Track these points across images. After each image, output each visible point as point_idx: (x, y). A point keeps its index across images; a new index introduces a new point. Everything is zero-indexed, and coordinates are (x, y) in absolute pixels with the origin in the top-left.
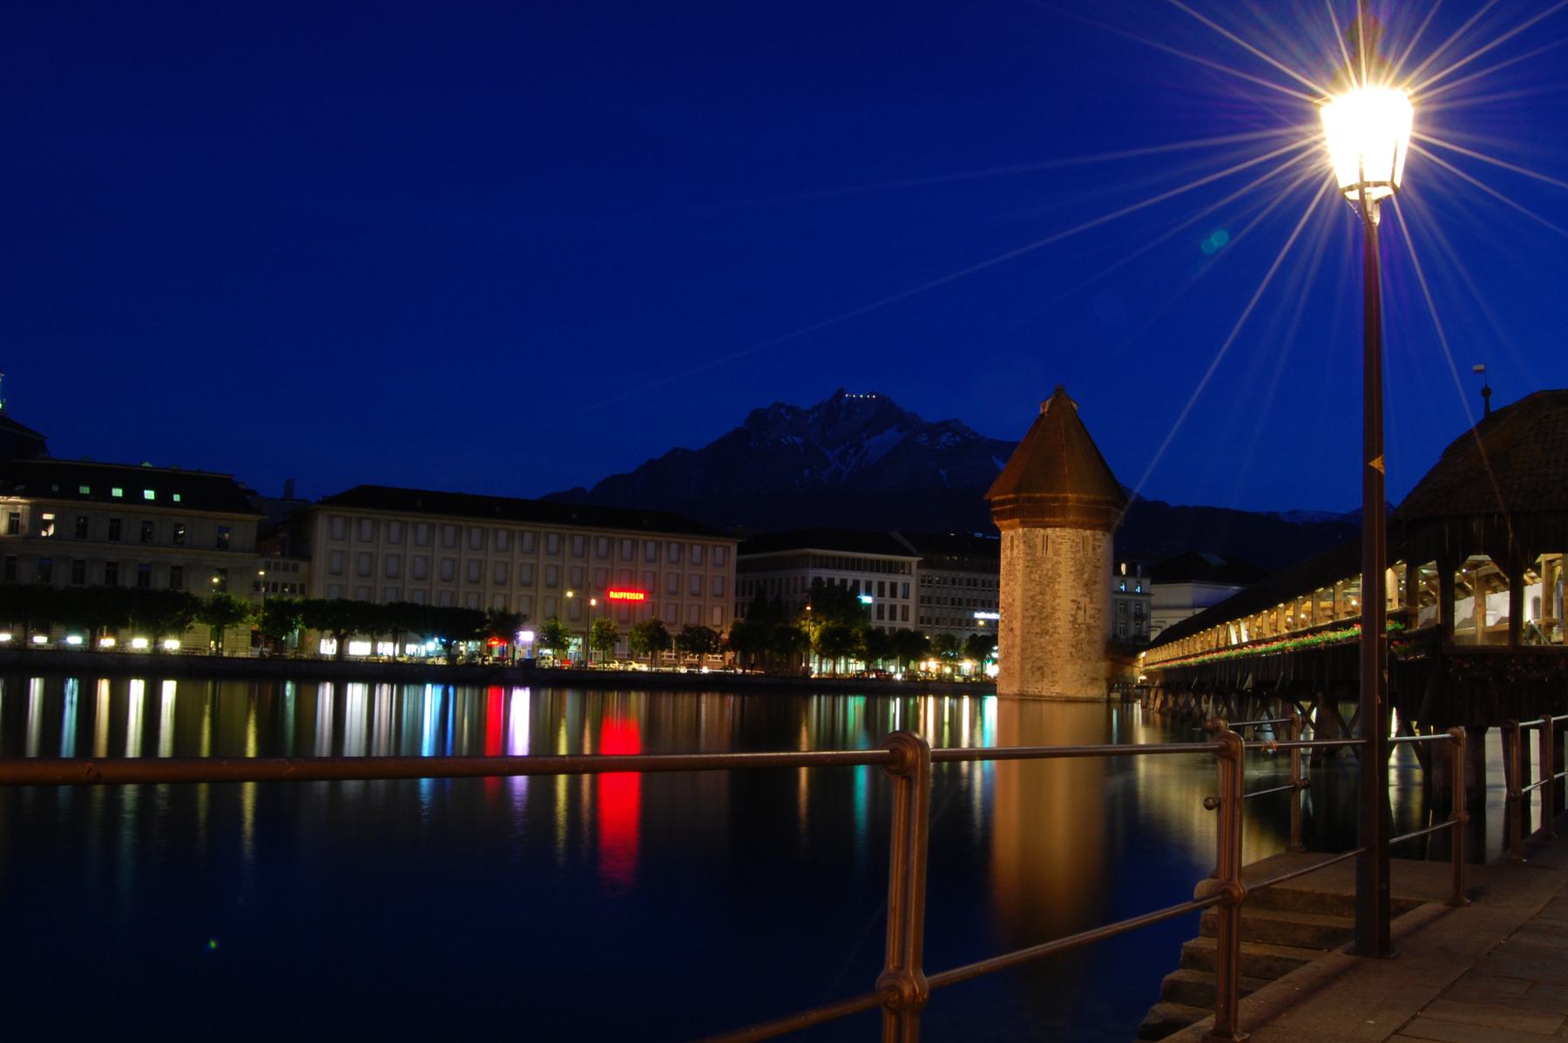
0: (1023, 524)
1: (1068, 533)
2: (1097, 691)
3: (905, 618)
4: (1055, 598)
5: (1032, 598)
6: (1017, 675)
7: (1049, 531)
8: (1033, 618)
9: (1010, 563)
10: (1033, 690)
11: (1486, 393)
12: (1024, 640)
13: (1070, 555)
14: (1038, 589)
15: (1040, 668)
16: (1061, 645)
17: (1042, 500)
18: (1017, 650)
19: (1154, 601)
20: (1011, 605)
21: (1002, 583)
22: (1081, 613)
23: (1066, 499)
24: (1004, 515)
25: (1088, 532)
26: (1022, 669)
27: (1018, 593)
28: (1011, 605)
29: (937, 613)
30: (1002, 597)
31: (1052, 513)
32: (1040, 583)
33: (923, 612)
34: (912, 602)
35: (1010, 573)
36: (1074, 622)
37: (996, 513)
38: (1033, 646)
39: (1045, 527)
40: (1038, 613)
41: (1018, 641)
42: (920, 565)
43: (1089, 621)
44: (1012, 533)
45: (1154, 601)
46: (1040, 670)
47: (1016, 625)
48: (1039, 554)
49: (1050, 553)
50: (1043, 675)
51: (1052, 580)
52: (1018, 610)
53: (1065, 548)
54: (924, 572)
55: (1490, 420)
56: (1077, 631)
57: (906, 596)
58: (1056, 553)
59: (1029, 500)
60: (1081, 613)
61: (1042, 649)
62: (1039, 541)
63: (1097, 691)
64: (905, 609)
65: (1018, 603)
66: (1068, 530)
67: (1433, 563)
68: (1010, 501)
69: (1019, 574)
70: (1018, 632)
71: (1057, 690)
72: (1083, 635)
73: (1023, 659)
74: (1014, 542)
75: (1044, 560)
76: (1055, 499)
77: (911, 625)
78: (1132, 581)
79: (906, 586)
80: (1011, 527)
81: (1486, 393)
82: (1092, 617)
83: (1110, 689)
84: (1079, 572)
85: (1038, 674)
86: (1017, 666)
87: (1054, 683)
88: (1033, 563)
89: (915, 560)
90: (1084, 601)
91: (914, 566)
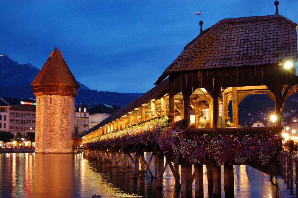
0: (44, 94)
1: (59, 97)
2: (69, 150)
3: (5, 127)
4: (54, 119)
5: (47, 119)
6: (42, 146)
7: (53, 96)
8: (47, 126)
9: (39, 108)
10: (47, 151)
11: (201, 23)
12: (44, 134)
13: (60, 104)
14: (49, 116)
15: (50, 143)
16: (56, 135)
17: (50, 86)
18: (42, 137)
19: (90, 120)
20: (39, 122)
21: (37, 114)
22: (64, 124)
23: (58, 86)
24: (37, 91)
25: (66, 97)
26: (44, 144)
27: (42, 118)
28: (39, 122)
29: (17, 125)
30: (36, 119)
31: (54, 90)
32: (50, 114)
33: (11, 125)
34: (7, 122)
35: (39, 110)
36: (61, 127)
37: (34, 90)
38: (47, 136)
39: (51, 95)
40: (49, 125)
41: (42, 134)
42: (10, 109)
43: (66, 126)
44: (40, 97)
46: (50, 144)
47: (41, 128)
48: (49, 104)
49: (53, 103)
50: (51, 145)
51: (54, 113)
52: (42, 123)
53: (58, 102)
54: (12, 111)
55: (203, 33)
56: (62, 130)
57: (5, 119)
58: (55, 104)
59: (46, 86)
60: (64, 124)
61: (50, 136)
62: (49, 100)
63: (69, 150)
64: (5, 124)
65: (42, 121)
66: (59, 96)
67: (181, 93)
68: (39, 86)
69: (42, 111)
70: (42, 131)
71: (55, 150)
72: (64, 131)
75: (51, 106)
76: (54, 86)
77: (7, 130)
79: (5, 116)
80: (40, 95)
81: (201, 23)
82: (67, 125)
83: (74, 149)
84: (63, 110)
86: (42, 143)
87: (54, 148)
88: (47, 107)
89: (8, 107)
90: (65, 120)
91: (8, 109)
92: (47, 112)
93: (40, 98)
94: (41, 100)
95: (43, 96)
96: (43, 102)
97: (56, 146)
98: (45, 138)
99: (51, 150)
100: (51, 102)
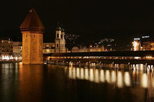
0: (30, 33)
5: (32, 46)
10: (32, 63)
12: (31, 54)
17: (35, 28)
18: (29, 56)
23: (39, 28)
31: (36, 31)
41: (29, 54)
45: (13, 45)
52: (29, 48)
53: (38, 37)
59: (32, 28)
68: (28, 28)
71: (37, 63)
73: (30, 57)
74: (26, 37)
76: (37, 28)
78: (11, 41)
80: (27, 33)
84: (40, 41)
85: (33, 60)
86: (29, 59)
90: (41, 46)
92: (32, 42)
93: (27, 35)
94: (28, 36)
95: (29, 34)
96: (30, 36)
97: (37, 60)
98: (31, 56)
99: (35, 62)
100: (34, 37)
